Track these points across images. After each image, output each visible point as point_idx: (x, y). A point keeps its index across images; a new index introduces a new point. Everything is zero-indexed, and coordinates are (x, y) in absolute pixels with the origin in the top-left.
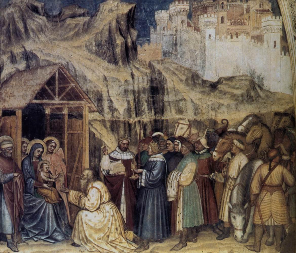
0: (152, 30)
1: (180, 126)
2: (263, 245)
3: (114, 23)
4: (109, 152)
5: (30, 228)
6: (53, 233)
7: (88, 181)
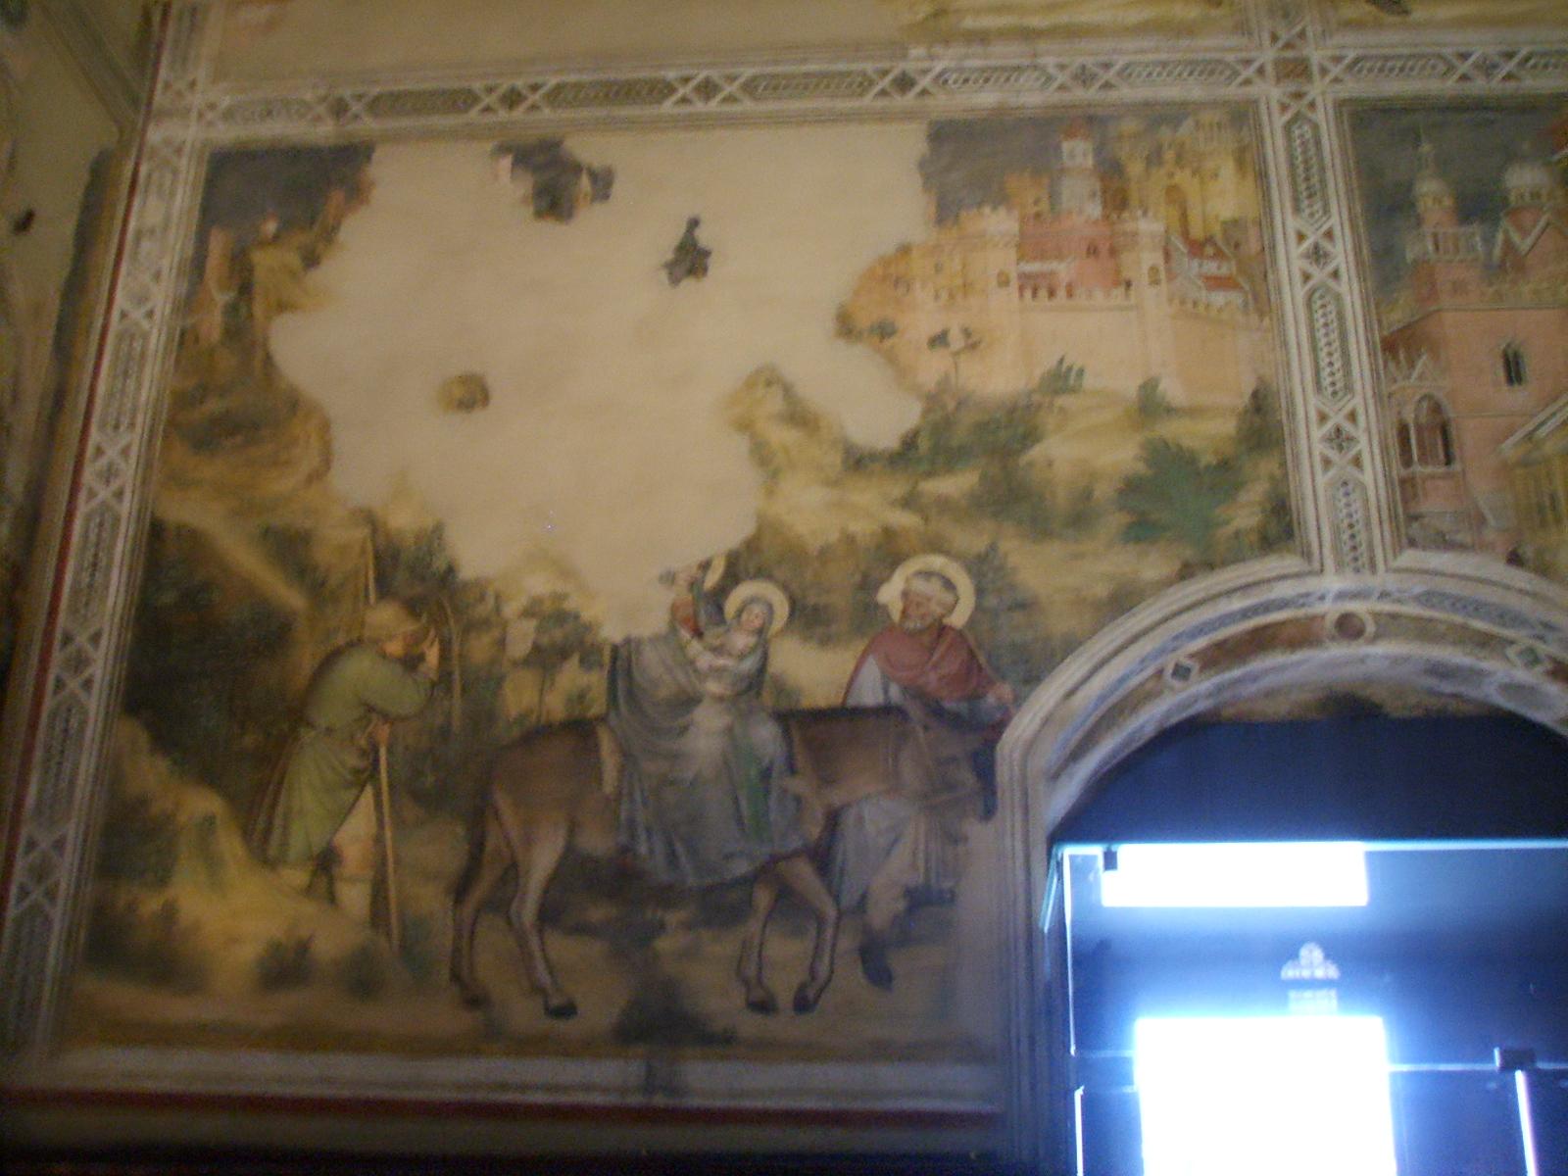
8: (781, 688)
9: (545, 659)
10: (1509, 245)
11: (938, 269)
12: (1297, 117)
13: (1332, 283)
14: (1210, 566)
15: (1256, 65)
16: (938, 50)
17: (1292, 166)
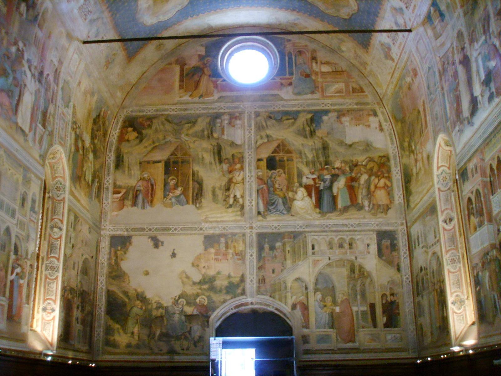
0: (322, 124)
3: (305, 122)
7: (297, 188)
8: (185, 312)
9: (158, 308)
10: (275, 255)
11: (205, 257)
14: (235, 297)
16: (206, 224)
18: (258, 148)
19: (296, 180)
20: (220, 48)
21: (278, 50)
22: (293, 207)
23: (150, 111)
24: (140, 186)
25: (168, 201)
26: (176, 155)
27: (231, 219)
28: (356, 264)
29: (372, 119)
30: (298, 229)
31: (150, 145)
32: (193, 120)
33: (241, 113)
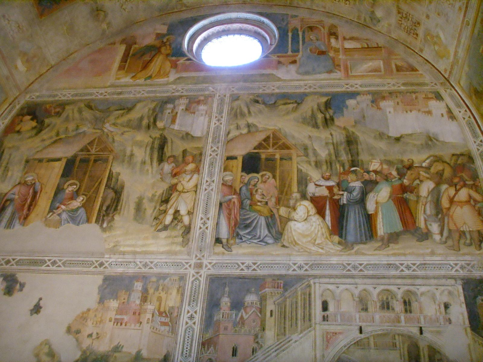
0: (345, 110)
1: (373, 164)
2: (462, 246)
3: (316, 107)
4: (314, 181)
5: (244, 234)
6: (265, 237)
7: (297, 201)
10: (242, 317)
11: (95, 316)
12: (197, 279)
13: (193, 325)
15: (189, 264)
16: (112, 256)
17: (191, 292)
18: (228, 142)
19: (295, 188)
20: (191, 26)
21: (276, 26)
22: (286, 232)
23: (65, 95)
24: (14, 194)
25: (55, 217)
26: (89, 151)
27: (162, 249)
28: (422, 345)
29: (433, 104)
30: (294, 270)
31: (51, 138)
32: (129, 106)
33: (207, 97)
